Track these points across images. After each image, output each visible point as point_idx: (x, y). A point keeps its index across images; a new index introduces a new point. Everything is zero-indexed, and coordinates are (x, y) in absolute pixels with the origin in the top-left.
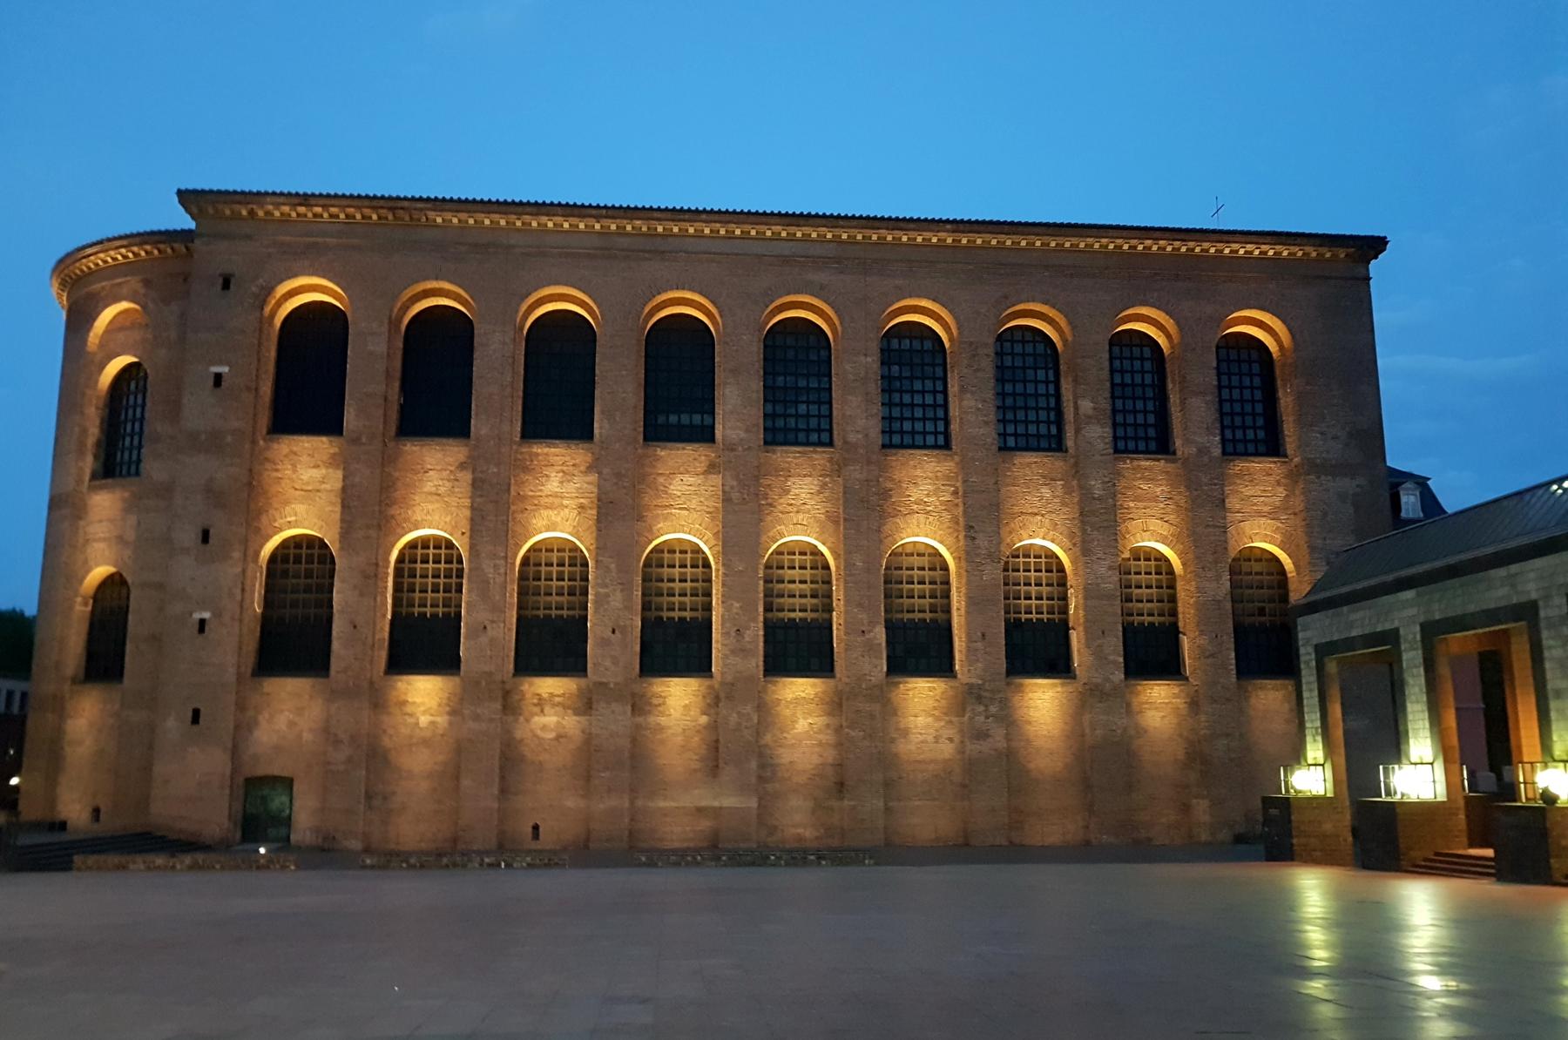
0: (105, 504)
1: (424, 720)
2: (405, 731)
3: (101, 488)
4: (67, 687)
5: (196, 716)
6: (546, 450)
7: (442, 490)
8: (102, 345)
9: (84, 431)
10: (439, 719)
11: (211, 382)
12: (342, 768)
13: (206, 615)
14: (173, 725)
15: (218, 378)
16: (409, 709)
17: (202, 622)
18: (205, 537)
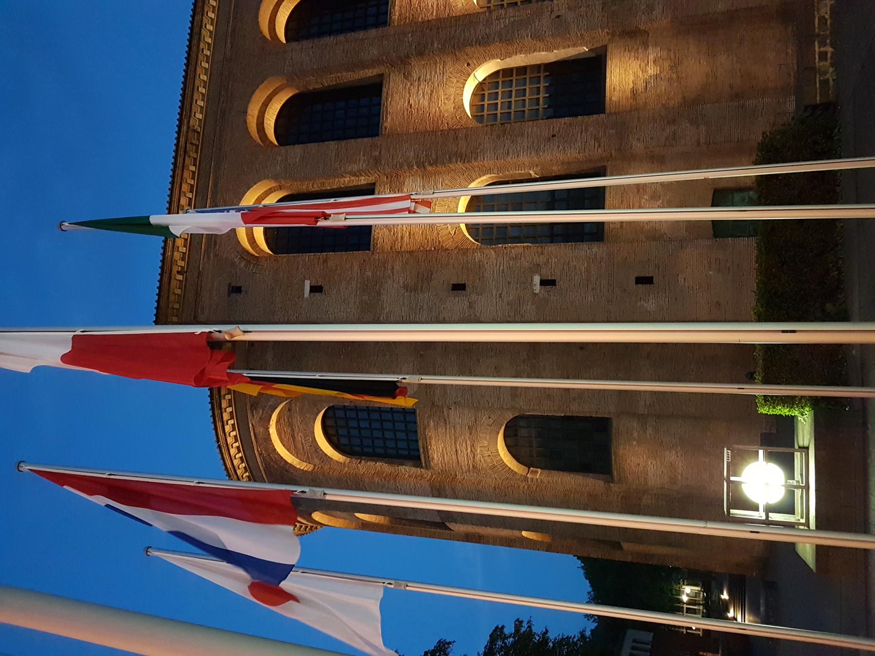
0: (441, 448)
1: (652, 70)
2: (663, 85)
3: (427, 457)
4: (615, 487)
5: (640, 280)
6: (397, 8)
7: (428, 90)
8: (308, 460)
9: (378, 474)
10: (651, 57)
12: (703, 128)
13: (537, 279)
15: (315, 289)
16: (641, 86)
17: (543, 283)
18: (459, 287)
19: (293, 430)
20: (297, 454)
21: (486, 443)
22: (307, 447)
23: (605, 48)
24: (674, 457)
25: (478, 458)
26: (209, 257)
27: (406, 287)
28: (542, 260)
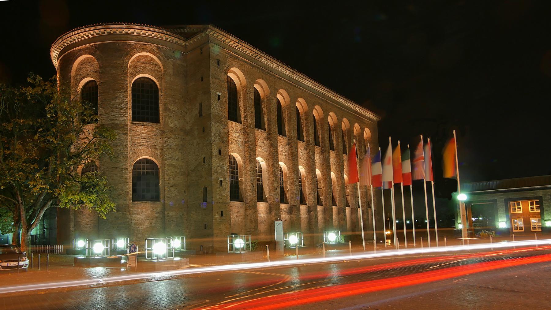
0: (143, 131)
1: (262, 215)
3: (138, 125)
4: (130, 202)
11: (217, 98)
12: (253, 230)
13: (222, 179)
14: (217, 216)
19: (147, 63)
20: (135, 62)
21: (147, 151)
22: (138, 68)
23: (267, 202)
24: (147, 224)
25: (140, 147)
26: (227, 53)
27: (220, 133)
28: (227, 181)
